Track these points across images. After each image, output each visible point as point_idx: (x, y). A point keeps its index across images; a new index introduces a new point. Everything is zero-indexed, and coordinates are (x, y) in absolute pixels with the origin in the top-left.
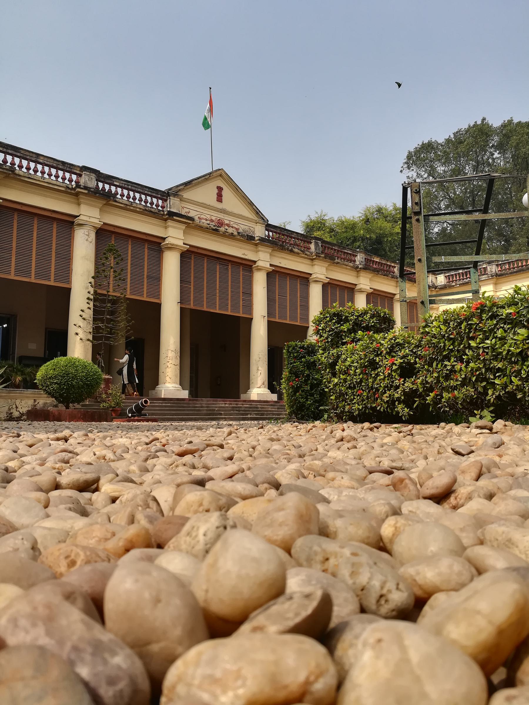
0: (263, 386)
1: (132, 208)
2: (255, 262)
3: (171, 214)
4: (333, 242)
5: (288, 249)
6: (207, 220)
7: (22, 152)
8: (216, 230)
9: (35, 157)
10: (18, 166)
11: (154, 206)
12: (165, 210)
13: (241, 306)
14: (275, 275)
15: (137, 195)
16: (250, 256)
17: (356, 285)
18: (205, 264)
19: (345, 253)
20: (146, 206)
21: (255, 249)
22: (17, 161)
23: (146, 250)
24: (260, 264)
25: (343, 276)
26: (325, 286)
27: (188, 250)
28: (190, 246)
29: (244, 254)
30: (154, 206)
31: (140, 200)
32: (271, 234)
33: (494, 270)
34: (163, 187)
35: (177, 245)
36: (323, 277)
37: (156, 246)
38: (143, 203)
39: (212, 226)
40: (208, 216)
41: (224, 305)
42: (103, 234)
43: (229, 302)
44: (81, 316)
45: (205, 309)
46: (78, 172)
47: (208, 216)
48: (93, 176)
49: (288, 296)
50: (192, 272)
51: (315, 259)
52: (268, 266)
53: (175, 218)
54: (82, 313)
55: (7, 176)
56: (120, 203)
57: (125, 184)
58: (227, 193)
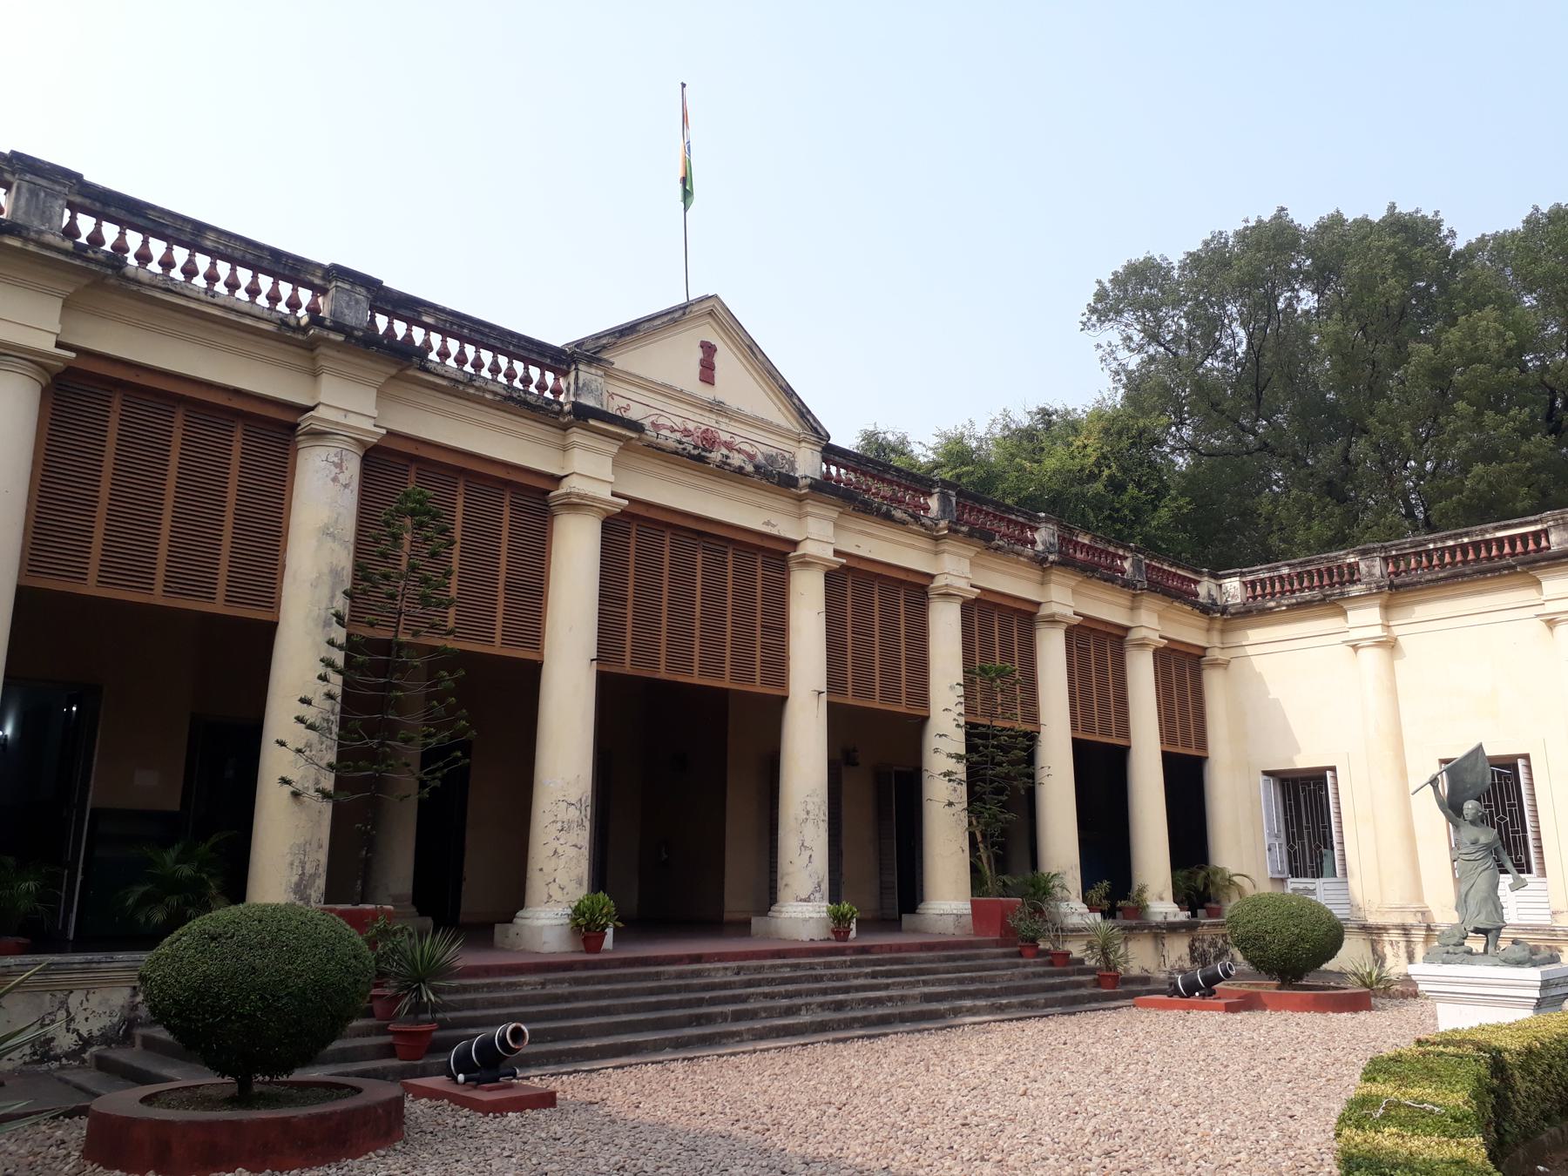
0: (818, 895)
1: (471, 391)
2: (794, 544)
3: (582, 414)
4: (980, 494)
5: (879, 509)
6: (673, 430)
7: (152, 215)
8: (701, 459)
9: (191, 233)
10: (137, 256)
11: (532, 388)
12: (562, 398)
13: (758, 663)
14: (848, 580)
15: (487, 356)
16: (783, 527)
17: (1039, 604)
18: (667, 551)
19: (1010, 521)
20: (510, 387)
21: (791, 508)
22: (134, 240)
23: (507, 511)
24: (808, 548)
25: (1012, 582)
26: (968, 608)
27: (623, 513)
28: (632, 500)
29: (768, 523)
30: (532, 388)
31: (495, 369)
32: (833, 469)
33: (1377, 571)
34: (558, 337)
35: (594, 499)
36: (963, 584)
37: (536, 499)
38: (501, 378)
39: (690, 448)
40: (678, 421)
41: (713, 664)
42: (385, 462)
43: (728, 652)
44: (300, 720)
45: (663, 674)
46: (317, 281)
47: (678, 421)
48: (361, 294)
49: (877, 633)
50: (632, 572)
51: (944, 537)
52: (829, 555)
53: (591, 422)
54: (304, 711)
55: (98, 282)
56: (437, 375)
57: (452, 324)
58: (726, 360)
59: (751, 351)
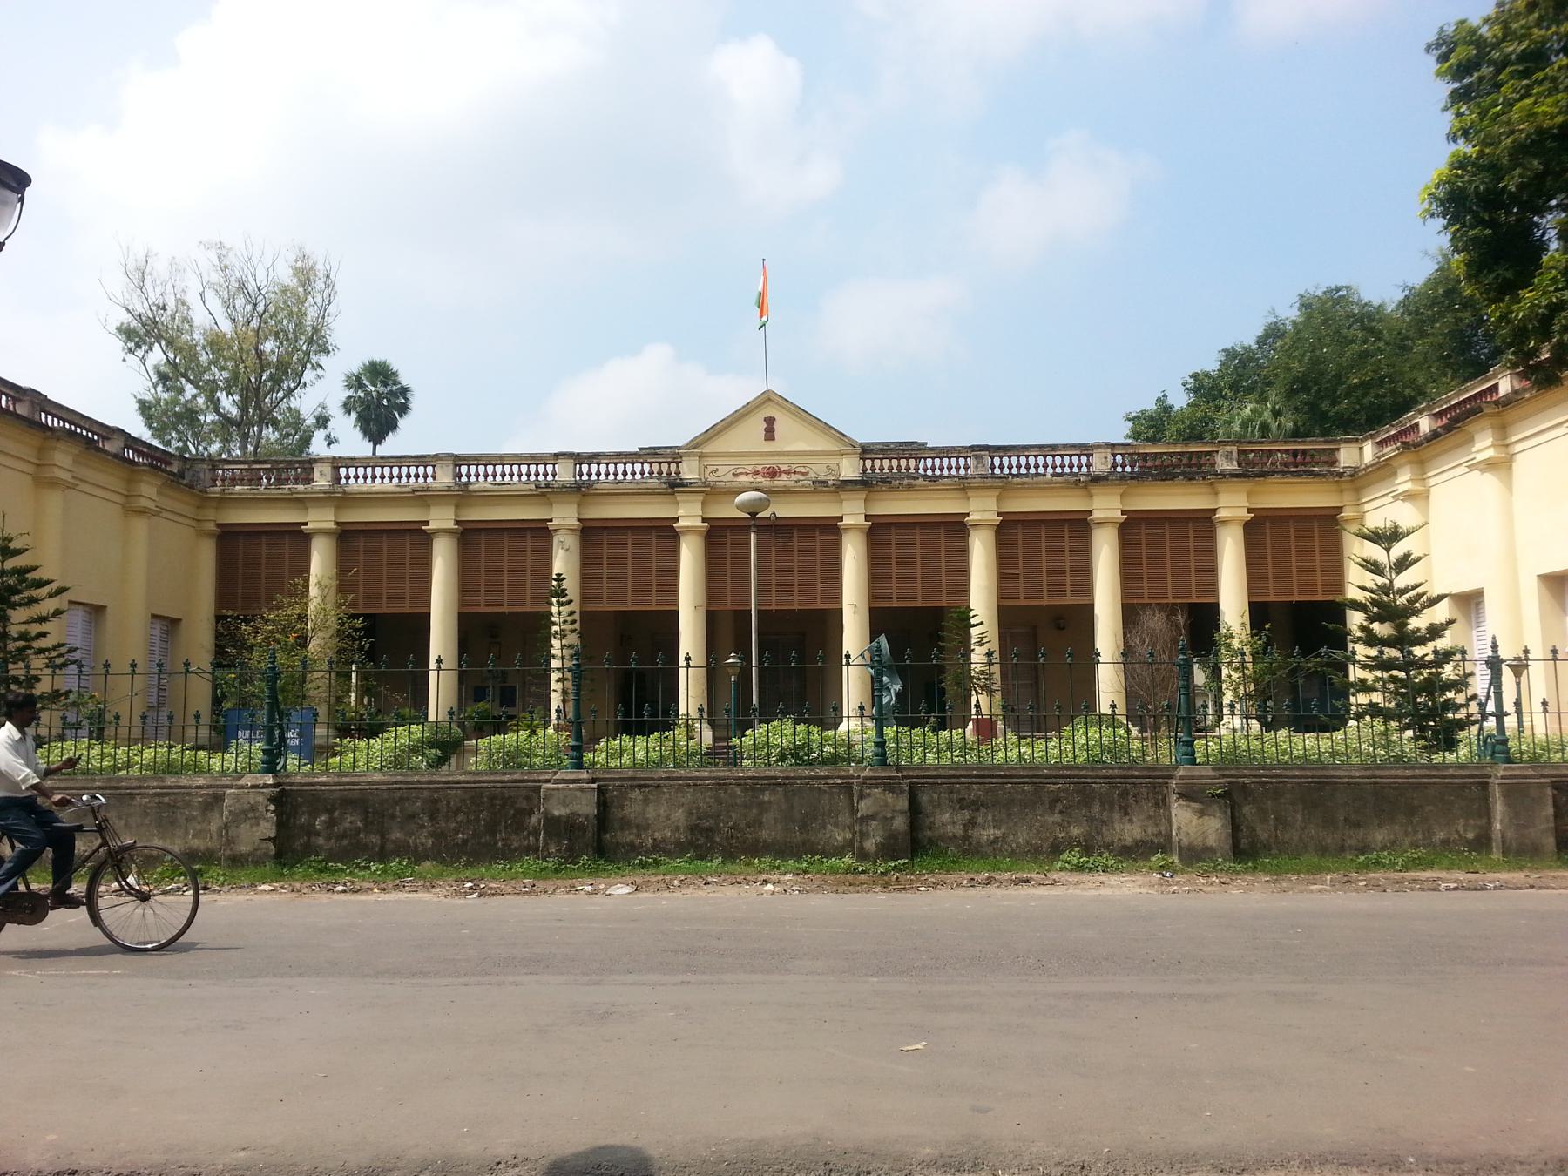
24: (847, 521)
48: (570, 463)
59: (800, 413)
